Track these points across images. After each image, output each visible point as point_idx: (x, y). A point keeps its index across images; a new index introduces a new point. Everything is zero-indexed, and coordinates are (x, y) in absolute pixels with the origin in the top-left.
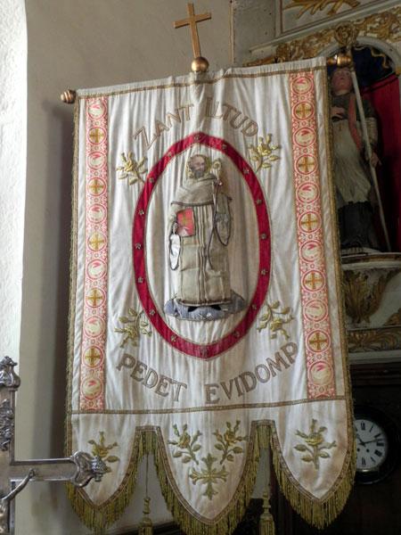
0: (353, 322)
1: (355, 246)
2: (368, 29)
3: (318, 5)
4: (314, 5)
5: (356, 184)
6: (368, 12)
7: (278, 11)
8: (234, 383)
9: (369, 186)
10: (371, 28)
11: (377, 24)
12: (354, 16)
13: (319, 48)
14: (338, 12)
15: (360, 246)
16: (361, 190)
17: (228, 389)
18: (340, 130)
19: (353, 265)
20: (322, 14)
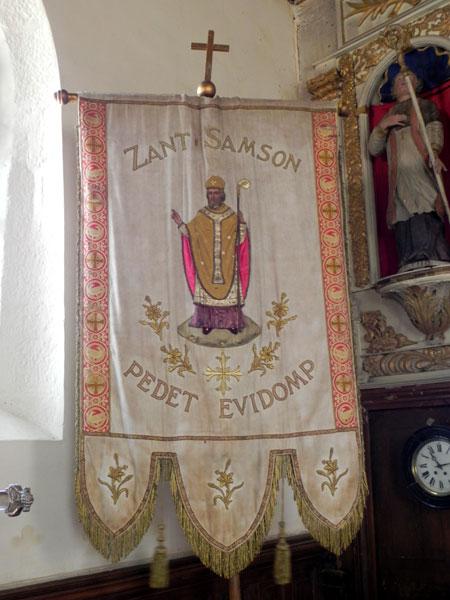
0: (427, 339)
1: (421, 260)
2: (430, 27)
3: (378, 9)
4: (374, 10)
5: (422, 195)
6: (430, 9)
7: (339, 19)
8: (249, 400)
9: (435, 195)
10: (433, 26)
11: (439, 21)
12: (412, 18)
13: (381, 54)
14: (399, 12)
15: (426, 259)
16: (426, 199)
17: (241, 406)
18: (403, 138)
19: (419, 279)
20: (383, 18)
